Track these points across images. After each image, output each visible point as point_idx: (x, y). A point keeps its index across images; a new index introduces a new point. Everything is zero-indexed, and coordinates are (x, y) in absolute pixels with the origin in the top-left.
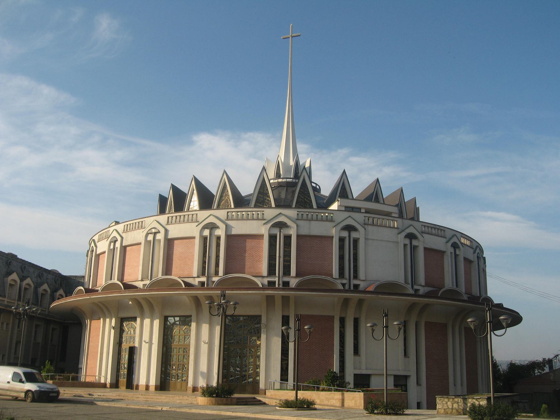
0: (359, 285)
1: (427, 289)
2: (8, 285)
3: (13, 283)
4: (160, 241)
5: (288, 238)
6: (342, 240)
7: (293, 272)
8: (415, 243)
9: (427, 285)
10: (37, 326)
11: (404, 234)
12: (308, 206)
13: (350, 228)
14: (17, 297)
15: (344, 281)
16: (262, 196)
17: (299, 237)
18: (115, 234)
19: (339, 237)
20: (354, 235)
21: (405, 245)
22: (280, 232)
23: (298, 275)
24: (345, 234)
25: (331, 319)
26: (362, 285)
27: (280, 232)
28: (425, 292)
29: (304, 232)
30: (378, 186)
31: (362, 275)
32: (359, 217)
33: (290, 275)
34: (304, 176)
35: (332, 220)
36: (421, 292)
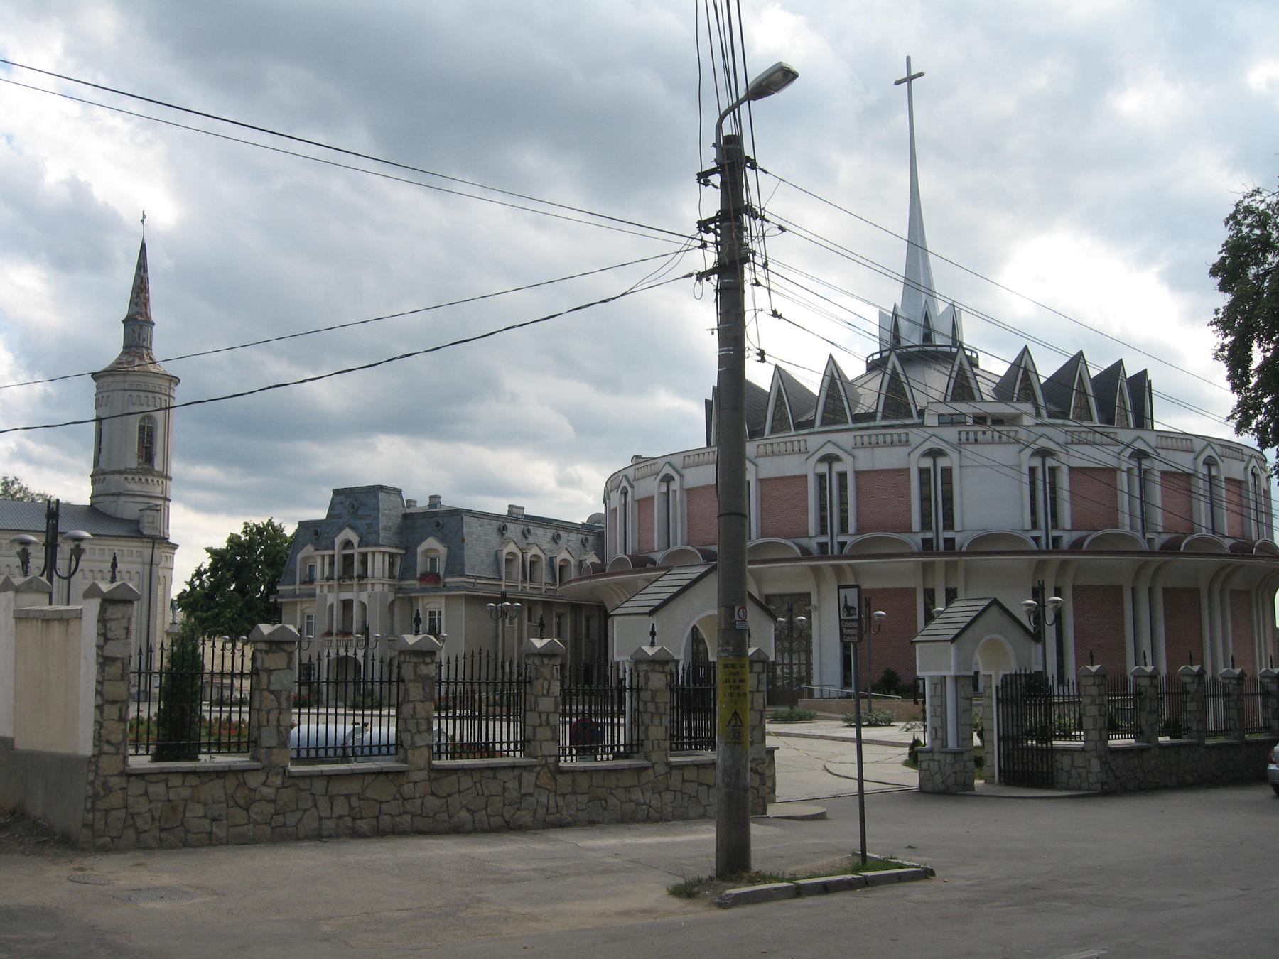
0: (953, 540)
1: (1076, 535)
2: (504, 561)
3: (510, 557)
4: (675, 491)
5: (842, 476)
6: (923, 472)
7: (852, 527)
8: (1050, 462)
9: (1075, 527)
10: (559, 616)
11: (1028, 452)
12: (903, 410)
13: (934, 453)
14: (520, 577)
15: (929, 535)
16: (832, 402)
17: (858, 474)
18: (624, 483)
19: (919, 468)
20: (942, 462)
21: (1032, 470)
22: (830, 469)
23: (859, 531)
24: (927, 463)
25: (911, 592)
26: (961, 540)
27: (830, 469)
28: (1073, 539)
29: (862, 466)
30: (1026, 360)
31: (957, 526)
32: (951, 433)
33: (847, 532)
34: (894, 363)
35: (907, 443)
36: (1065, 543)
